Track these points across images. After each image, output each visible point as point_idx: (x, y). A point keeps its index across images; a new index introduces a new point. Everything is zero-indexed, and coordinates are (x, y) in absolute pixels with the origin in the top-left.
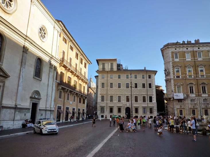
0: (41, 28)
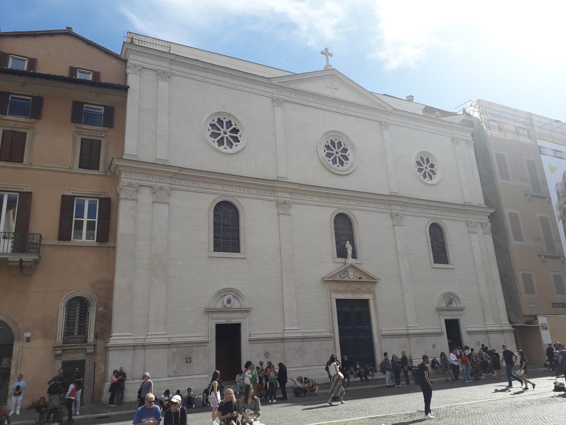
0: (419, 160)
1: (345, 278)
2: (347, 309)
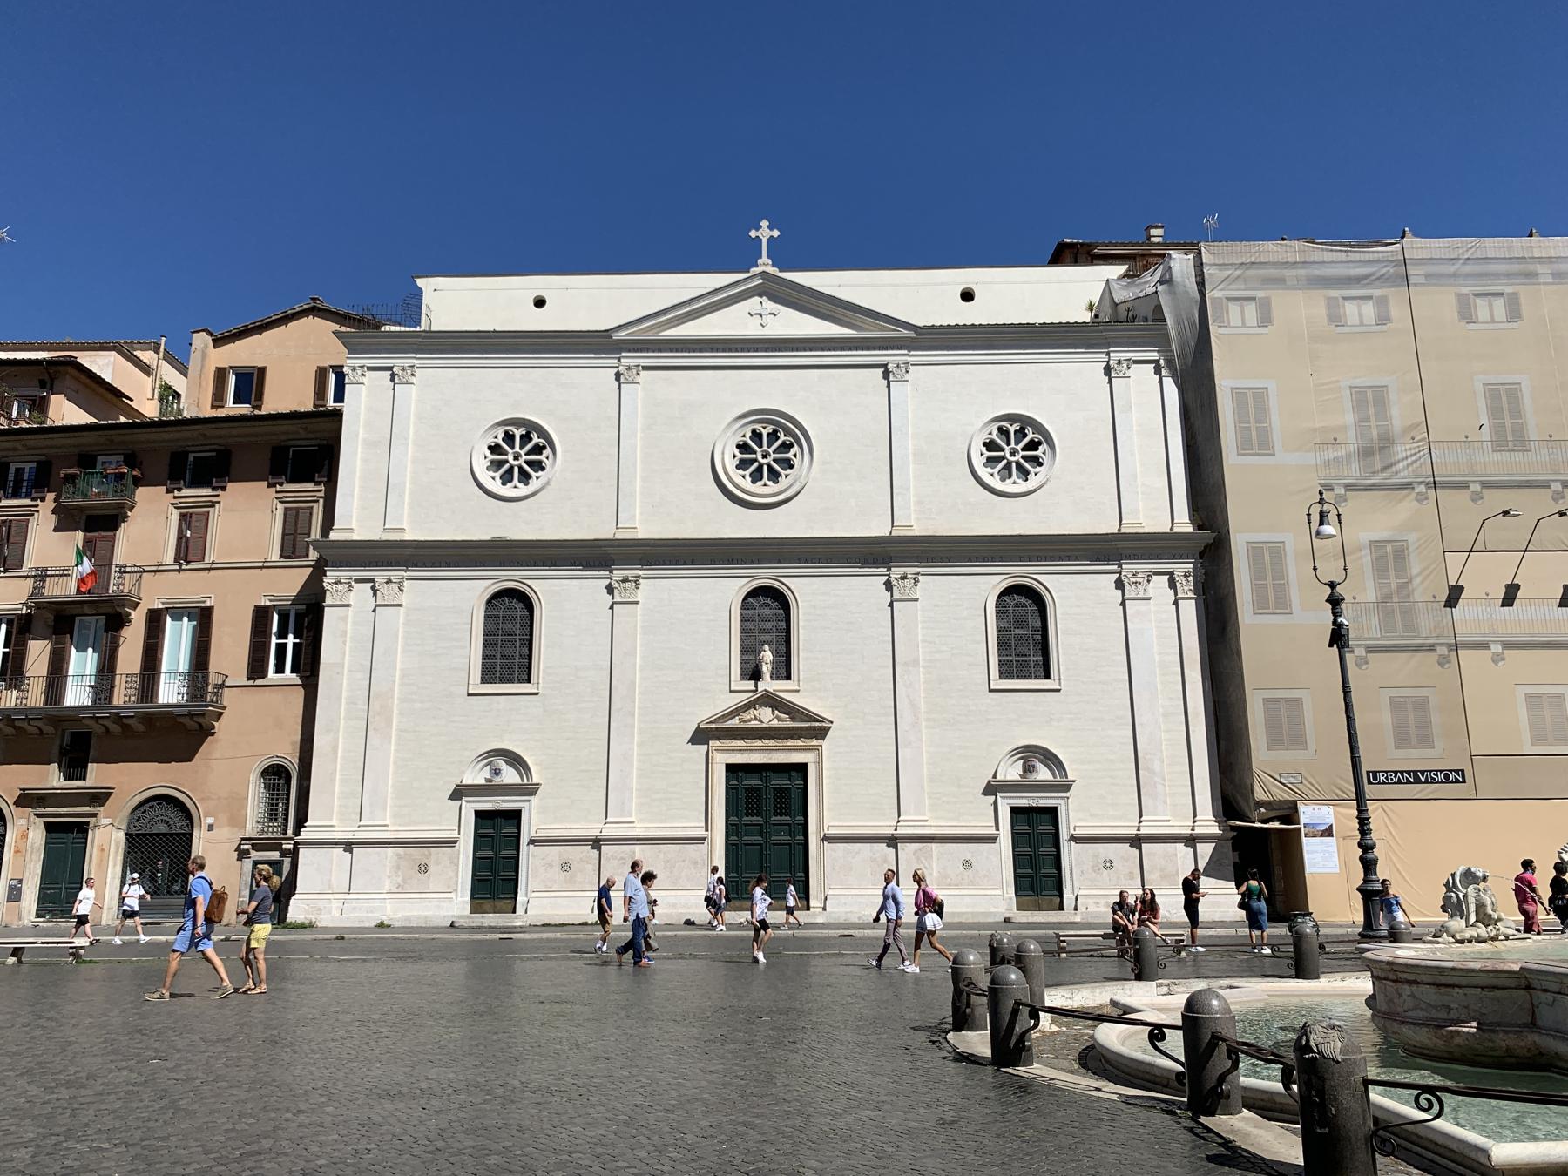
1: (752, 722)
2: (753, 783)
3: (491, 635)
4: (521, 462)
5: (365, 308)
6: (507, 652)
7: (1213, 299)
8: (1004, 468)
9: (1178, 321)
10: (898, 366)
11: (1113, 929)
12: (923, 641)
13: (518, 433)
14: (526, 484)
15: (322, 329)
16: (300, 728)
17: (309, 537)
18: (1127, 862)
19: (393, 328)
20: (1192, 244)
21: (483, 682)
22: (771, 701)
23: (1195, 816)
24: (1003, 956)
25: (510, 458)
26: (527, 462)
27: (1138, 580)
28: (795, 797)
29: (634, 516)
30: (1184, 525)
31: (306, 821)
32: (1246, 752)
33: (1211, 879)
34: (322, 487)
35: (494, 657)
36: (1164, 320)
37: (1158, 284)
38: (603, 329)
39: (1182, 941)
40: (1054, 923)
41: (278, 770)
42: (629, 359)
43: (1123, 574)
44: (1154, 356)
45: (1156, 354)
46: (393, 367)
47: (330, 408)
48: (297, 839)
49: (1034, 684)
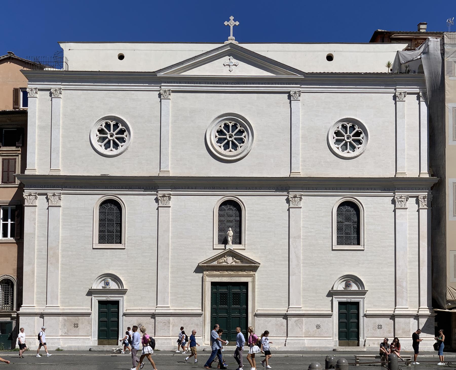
1: (223, 263)
3: (102, 221)
4: (114, 138)
5: (35, 58)
6: (110, 229)
7: (448, 62)
8: (343, 145)
9: (430, 73)
10: (295, 93)
11: (380, 354)
12: (303, 227)
13: (112, 124)
14: (117, 149)
15: (16, 68)
16: (16, 262)
17: (15, 173)
18: (388, 325)
19: (50, 69)
20: (440, 33)
21: (100, 243)
22: (232, 254)
23: (419, 306)
24: (331, 365)
25: (109, 136)
26: (116, 138)
27: (402, 200)
28: (243, 297)
29: (168, 165)
30: (425, 174)
31: (22, 304)
32: (444, 278)
33: (424, 333)
34: (20, 149)
35: (104, 231)
36: (423, 73)
37: (422, 54)
38: (153, 71)
39: (410, 360)
40: (355, 351)
41: (7, 282)
42: (165, 87)
43: (396, 197)
44: (417, 90)
45: (418, 90)
46: (50, 89)
47: (21, 109)
48: (18, 312)
49: (352, 247)
